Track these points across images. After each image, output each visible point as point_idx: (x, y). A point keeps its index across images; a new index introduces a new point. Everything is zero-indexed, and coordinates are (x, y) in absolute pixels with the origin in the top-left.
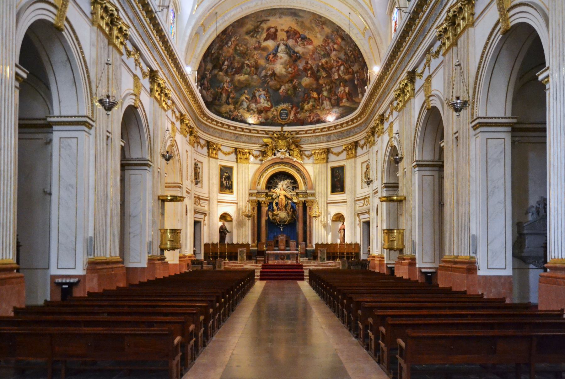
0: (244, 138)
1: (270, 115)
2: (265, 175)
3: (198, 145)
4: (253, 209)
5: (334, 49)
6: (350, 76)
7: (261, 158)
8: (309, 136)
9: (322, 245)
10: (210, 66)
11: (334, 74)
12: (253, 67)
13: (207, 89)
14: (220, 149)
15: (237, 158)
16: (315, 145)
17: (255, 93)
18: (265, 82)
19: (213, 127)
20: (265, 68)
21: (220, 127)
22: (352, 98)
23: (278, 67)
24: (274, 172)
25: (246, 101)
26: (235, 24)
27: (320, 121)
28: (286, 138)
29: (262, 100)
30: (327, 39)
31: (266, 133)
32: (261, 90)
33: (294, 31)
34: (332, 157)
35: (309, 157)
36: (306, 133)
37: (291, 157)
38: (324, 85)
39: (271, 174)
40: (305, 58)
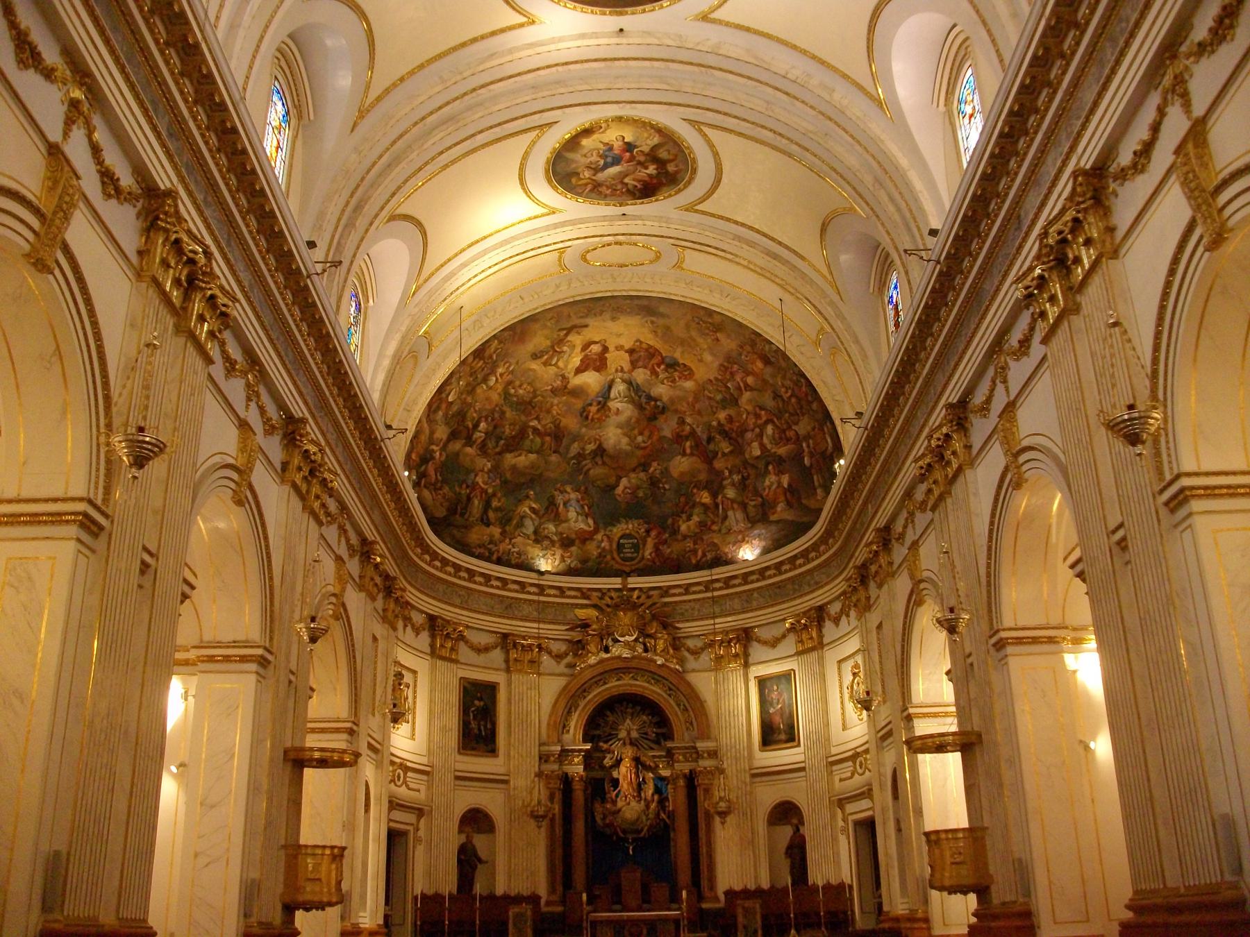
0: (527, 610)
1: (592, 549)
2: (582, 704)
3: (405, 626)
4: (551, 797)
5: (746, 385)
6: (790, 447)
7: (569, 659)
8: (694, 600)
9: (746, 894)
10: (442, 433)
11: (749, 444)
12: (549, 435)
13: (434, 487)
14: (462, 637)
15: (507, 661)
16: (712, 622)
17: (553, 497)
18: (578, 469)
19: (447, 581)
20: (576, 437)
21: (465, 580)
22: (799, 499)
23: (610, 434)
24: (606, 695)
25: (531, 518)
26: (506, 334)
27: (720, 561)
28: (635, 607)
29: (572, 514)
30: (729, 364)
31: (584, 594)
32: (568, 489)
33: (647, 350)
34: (757, 651)
35: (696, 653)
36: (687, 592)
37: (649, 655)
38: (727, 473)
39: (600, 699)
40: (676, 411)
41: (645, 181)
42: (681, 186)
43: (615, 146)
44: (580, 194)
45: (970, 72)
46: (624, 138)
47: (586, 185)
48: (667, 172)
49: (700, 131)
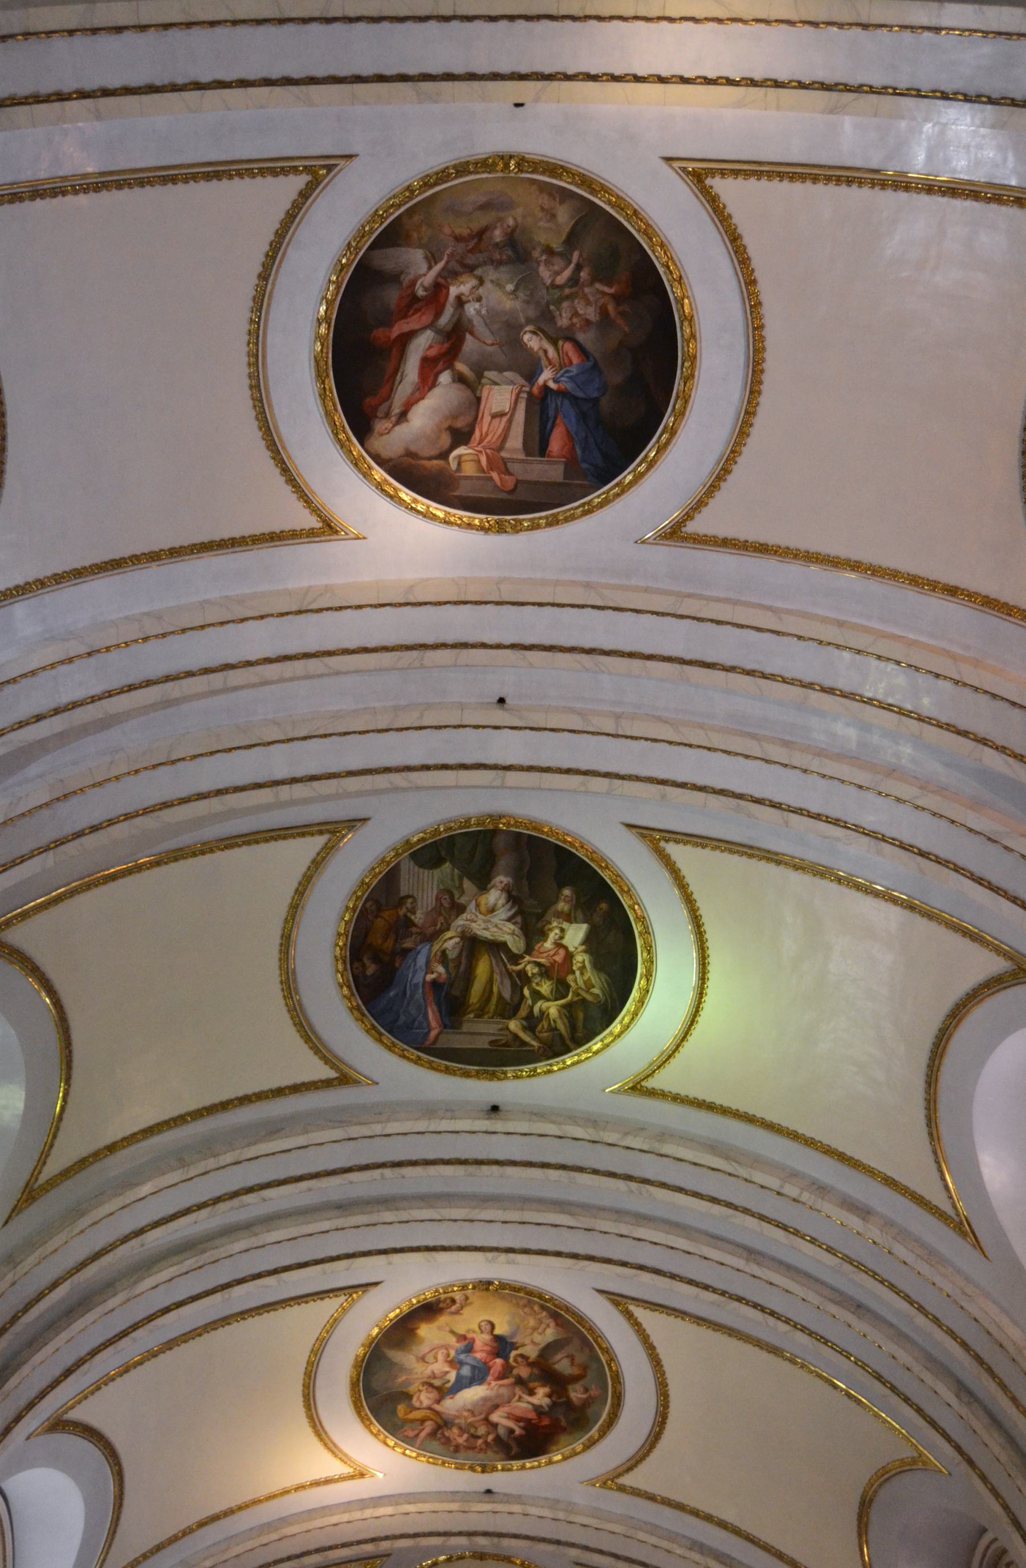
41: (528, 1421)
42: (594, 1432)
43: (478, 1345)
44: (409, 1441)
46: (493, 1326)
47: (423, 1421)
48: (569, 1403)
49: (629, 1316)
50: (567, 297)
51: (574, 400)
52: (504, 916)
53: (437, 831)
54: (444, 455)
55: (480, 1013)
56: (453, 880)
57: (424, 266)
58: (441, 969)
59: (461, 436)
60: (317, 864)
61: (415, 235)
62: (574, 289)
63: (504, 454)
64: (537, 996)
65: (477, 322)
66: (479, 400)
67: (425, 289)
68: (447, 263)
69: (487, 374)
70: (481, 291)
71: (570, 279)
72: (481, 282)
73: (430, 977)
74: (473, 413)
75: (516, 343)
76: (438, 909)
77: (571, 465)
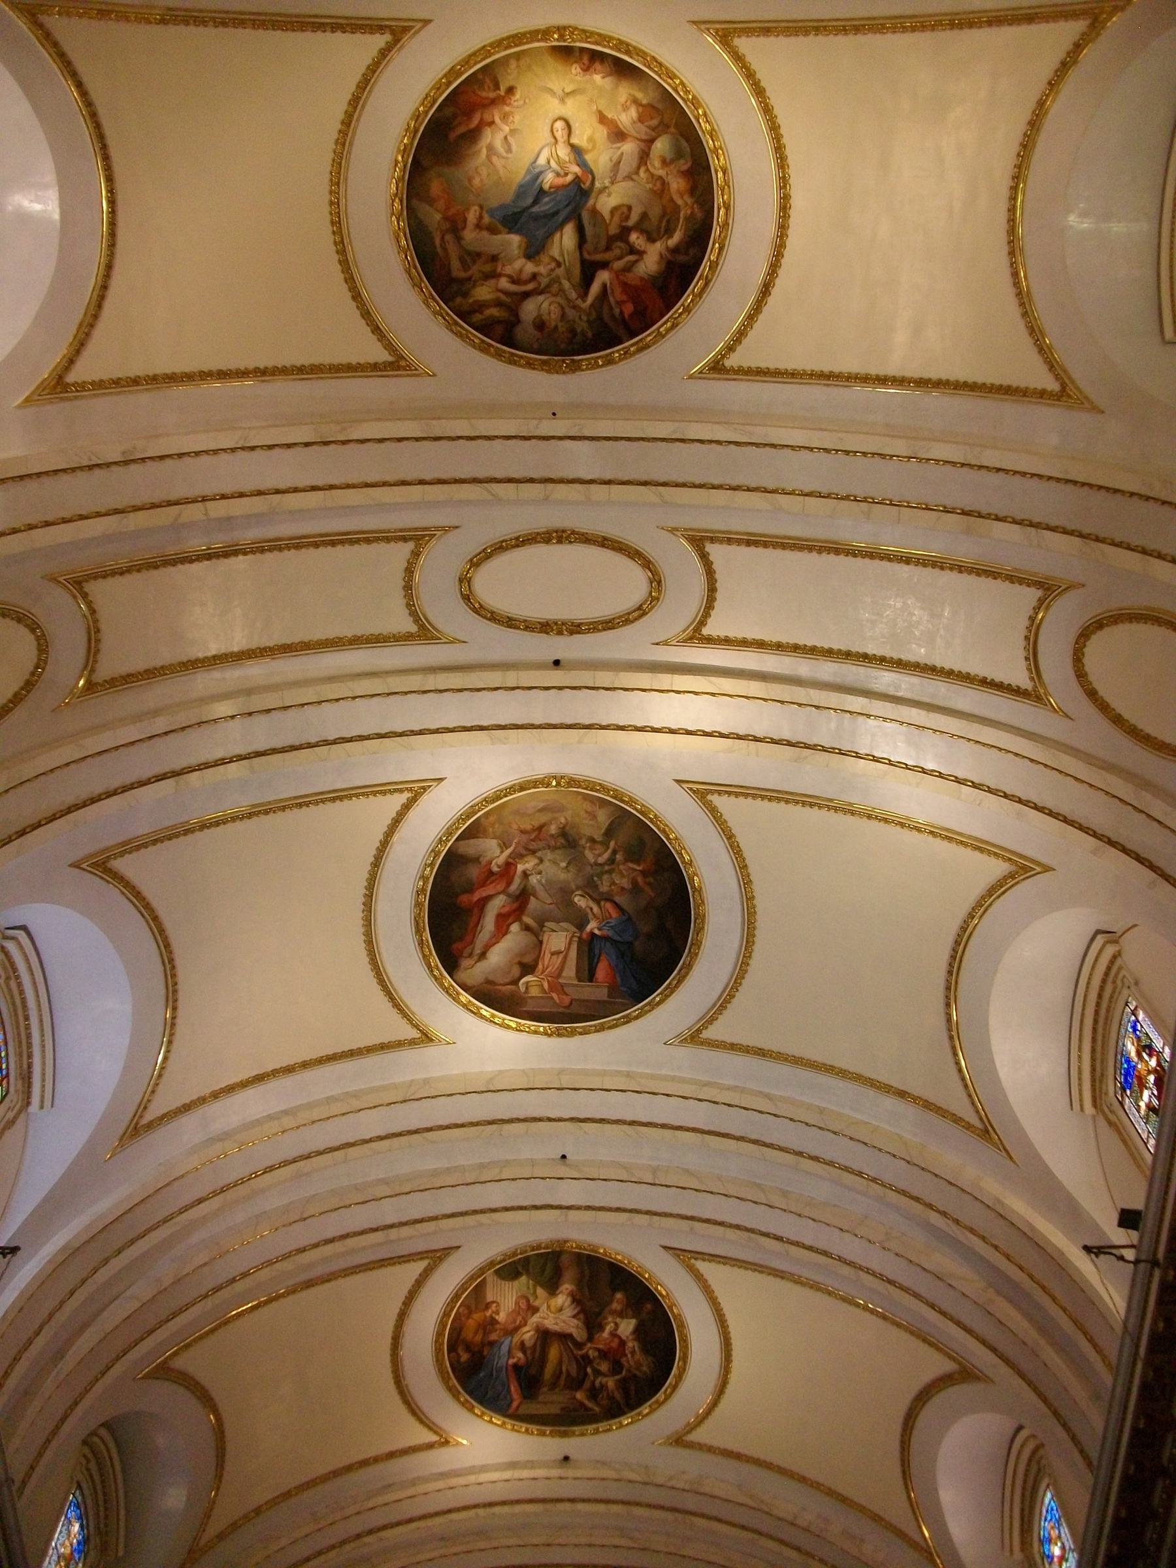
45: (1049, 1495)
50: (606, 872)
51: (614, 942)
52: (569, 1314)
53: (515, 1254)
54: (515, 982)
55: (554, 1386)
56: (528, 1288)
57: (498, 851)
58: (520, 1355)
59: (527, 969)
60: (419, 1283)
61: (491, 830)
62: (612, 867)
63: (561, 981)
64: (597, 1373)
65: (539, 889)
66: (541, 942)
67: (499, 867)
68: (515, 848)
69: (546, 924)
70: (541, 867)
71: (609, 859)
72: (541, 860)
73: (511, 1361)
74: (537, 953)
75: (571, 903)
76: (517, 1311)
77: (613, 990)
